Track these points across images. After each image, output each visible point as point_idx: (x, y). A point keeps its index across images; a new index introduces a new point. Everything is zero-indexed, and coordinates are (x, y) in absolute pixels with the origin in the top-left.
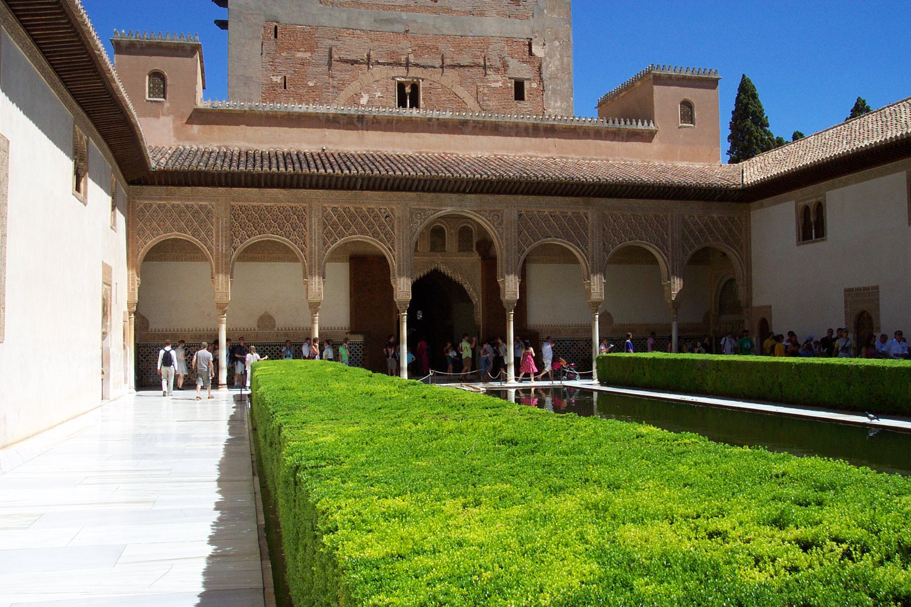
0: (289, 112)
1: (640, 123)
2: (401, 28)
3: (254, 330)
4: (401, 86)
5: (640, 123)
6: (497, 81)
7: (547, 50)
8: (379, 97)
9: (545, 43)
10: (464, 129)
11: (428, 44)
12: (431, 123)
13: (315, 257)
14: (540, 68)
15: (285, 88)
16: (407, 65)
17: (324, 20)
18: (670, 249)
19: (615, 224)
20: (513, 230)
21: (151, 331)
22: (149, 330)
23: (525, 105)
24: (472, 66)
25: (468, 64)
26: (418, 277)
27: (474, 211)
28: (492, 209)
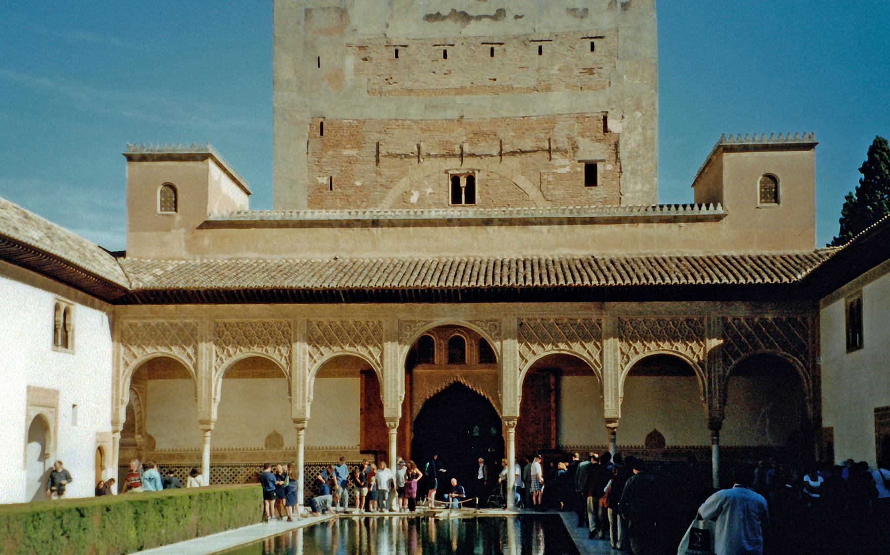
0: (301, 220)
1: (704, 207)
4: (455, 179)
5: (704, 207)
6: (564, 166)
7: (626, 123)
8: (430, 194)
9: (626, 116)
11: (484, 129)
14: (616, 145)
15: (331, 189)
17: (371, 112)
19: (636, 331)
23: (599, 191)
24: (535, 151)
26: (436, 392)
27: (470, 322)
28: (489, 318)
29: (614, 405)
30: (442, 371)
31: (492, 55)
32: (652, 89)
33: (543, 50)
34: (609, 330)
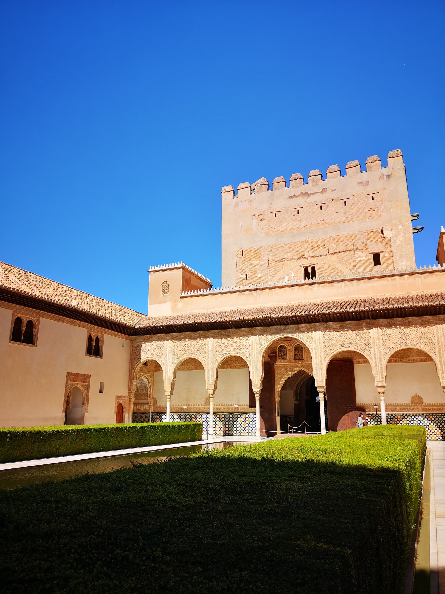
2: (303, 239)
3: (203, 405)
4: (306, 269)
6: (362, 257)
8: (293, 277)
9: (394, 229)
10: (312, 289)
12: (292, 288)
13: (210, 366)
15: (247, 280)
16: (308, 258)
18: (437, 349)
20: (319, 344)
21: (158, 406)
22: (157, 406)
24: (346, 251)
25: (343, 250)
29: (381, 380)
30: (291, 363)
31: (321, 209)
32: (407, 214)
33: (347, 203)
34: (375, 335)
